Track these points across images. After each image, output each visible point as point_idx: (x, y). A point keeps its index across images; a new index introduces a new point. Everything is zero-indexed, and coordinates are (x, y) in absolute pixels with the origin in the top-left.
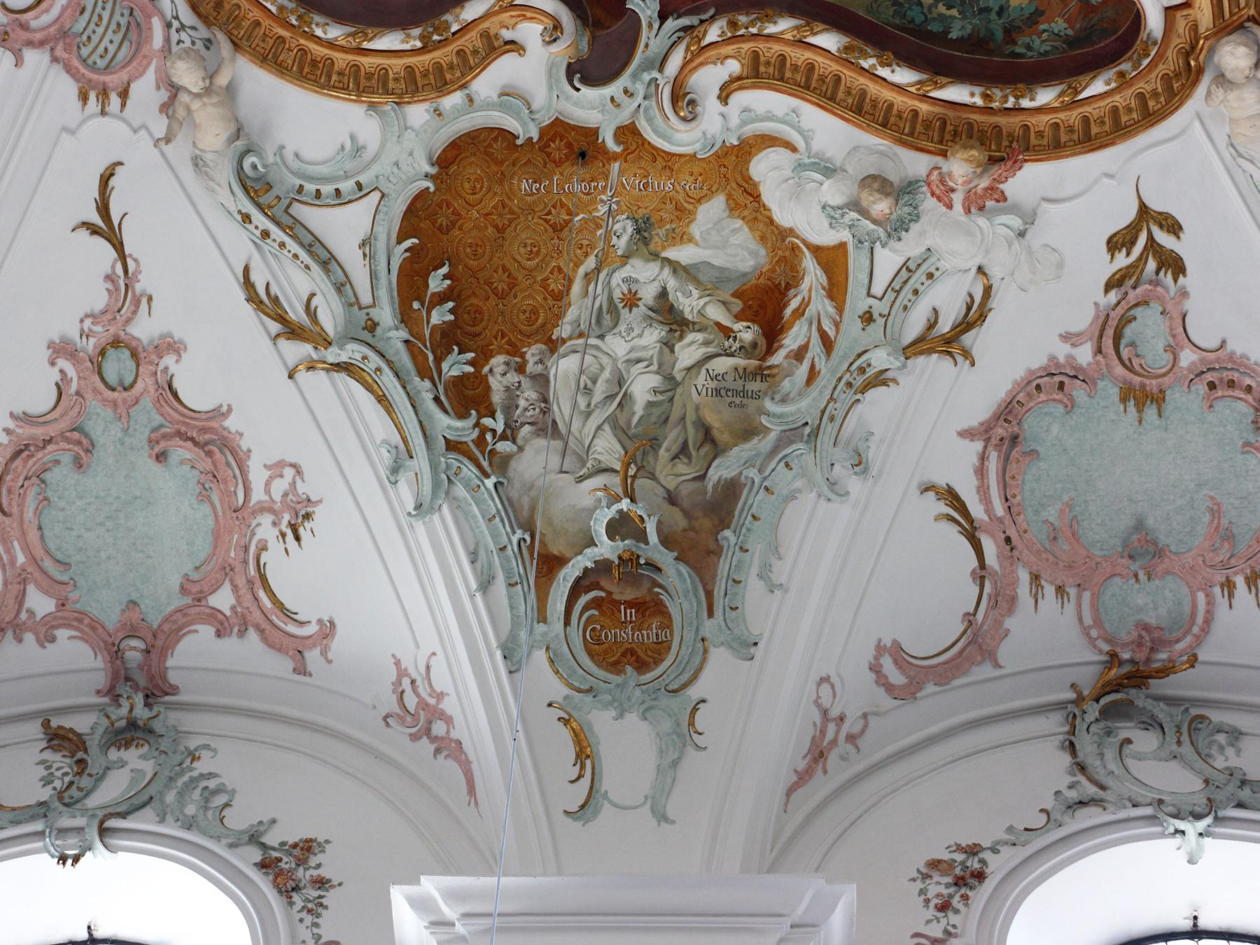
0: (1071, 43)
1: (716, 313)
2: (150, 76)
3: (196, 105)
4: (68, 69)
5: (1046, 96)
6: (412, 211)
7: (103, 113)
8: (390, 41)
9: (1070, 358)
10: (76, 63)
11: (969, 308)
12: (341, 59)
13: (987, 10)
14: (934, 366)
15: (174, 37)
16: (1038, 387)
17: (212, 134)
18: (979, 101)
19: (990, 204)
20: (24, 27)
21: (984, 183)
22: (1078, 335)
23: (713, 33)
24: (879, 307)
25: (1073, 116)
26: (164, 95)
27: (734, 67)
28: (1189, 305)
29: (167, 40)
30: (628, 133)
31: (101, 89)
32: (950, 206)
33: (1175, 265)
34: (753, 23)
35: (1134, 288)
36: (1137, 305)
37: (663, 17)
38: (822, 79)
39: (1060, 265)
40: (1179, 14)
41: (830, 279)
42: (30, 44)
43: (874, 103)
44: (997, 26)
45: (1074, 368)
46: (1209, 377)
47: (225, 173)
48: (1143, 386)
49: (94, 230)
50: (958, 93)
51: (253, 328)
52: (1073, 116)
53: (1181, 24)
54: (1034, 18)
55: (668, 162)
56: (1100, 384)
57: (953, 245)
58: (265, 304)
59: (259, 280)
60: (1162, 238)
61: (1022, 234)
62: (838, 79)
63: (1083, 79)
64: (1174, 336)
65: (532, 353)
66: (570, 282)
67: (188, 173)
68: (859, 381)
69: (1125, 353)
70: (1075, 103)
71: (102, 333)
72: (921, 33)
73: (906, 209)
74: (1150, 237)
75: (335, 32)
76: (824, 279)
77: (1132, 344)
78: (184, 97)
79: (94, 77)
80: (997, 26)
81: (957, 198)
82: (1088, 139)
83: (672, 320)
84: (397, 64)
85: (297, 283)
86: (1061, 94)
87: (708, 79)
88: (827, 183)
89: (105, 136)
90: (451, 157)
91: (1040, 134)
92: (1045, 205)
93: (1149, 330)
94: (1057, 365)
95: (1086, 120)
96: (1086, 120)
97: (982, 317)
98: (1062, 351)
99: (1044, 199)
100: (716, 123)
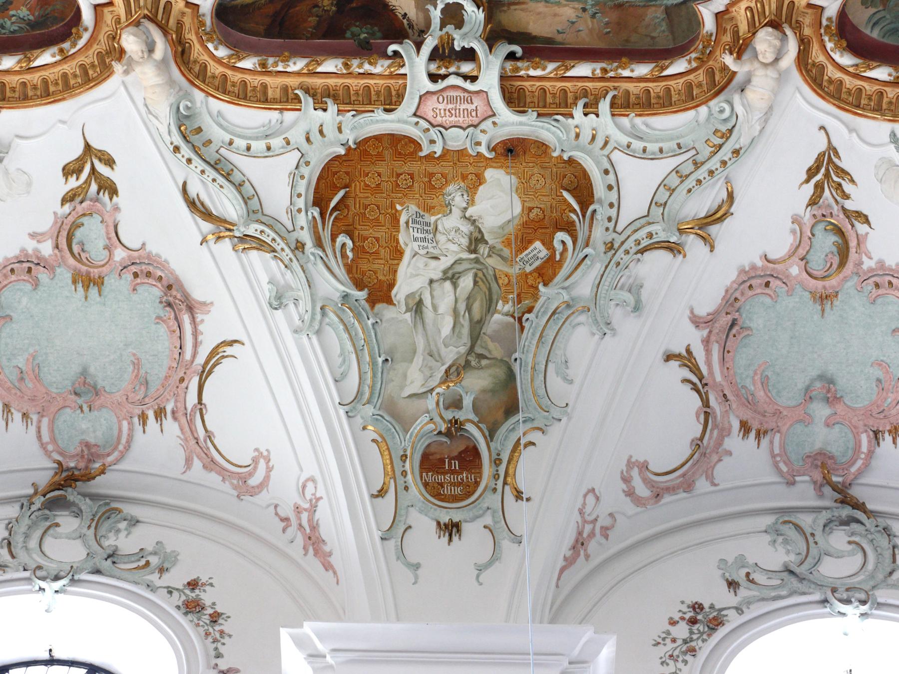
0: (33, 25)
9: (36, 251)
16: (12, 270)
22: (42, 234)
25: (35, 78)
28: (121, 217)
35: (81, 202)
36: (84, 215)
39: (29, 184)
40: (106, 10)
45: (38, 258)
46: (134, 269)
48: (88, 273)
53: (108, 17)
56: (58, 270)
60: (101, 168)
63: (36, 52)
64: (109, 239)
69: (76, 249)
74: (93, 169)
77: (82, 244)
82: (47, 93)
86: (19, 62)
91: (13, 90)
93: (93, 233)
94: (27, 255)
95: (45, 82)
96: (45, 82)
98: (30, 246)
99: (17, 136)
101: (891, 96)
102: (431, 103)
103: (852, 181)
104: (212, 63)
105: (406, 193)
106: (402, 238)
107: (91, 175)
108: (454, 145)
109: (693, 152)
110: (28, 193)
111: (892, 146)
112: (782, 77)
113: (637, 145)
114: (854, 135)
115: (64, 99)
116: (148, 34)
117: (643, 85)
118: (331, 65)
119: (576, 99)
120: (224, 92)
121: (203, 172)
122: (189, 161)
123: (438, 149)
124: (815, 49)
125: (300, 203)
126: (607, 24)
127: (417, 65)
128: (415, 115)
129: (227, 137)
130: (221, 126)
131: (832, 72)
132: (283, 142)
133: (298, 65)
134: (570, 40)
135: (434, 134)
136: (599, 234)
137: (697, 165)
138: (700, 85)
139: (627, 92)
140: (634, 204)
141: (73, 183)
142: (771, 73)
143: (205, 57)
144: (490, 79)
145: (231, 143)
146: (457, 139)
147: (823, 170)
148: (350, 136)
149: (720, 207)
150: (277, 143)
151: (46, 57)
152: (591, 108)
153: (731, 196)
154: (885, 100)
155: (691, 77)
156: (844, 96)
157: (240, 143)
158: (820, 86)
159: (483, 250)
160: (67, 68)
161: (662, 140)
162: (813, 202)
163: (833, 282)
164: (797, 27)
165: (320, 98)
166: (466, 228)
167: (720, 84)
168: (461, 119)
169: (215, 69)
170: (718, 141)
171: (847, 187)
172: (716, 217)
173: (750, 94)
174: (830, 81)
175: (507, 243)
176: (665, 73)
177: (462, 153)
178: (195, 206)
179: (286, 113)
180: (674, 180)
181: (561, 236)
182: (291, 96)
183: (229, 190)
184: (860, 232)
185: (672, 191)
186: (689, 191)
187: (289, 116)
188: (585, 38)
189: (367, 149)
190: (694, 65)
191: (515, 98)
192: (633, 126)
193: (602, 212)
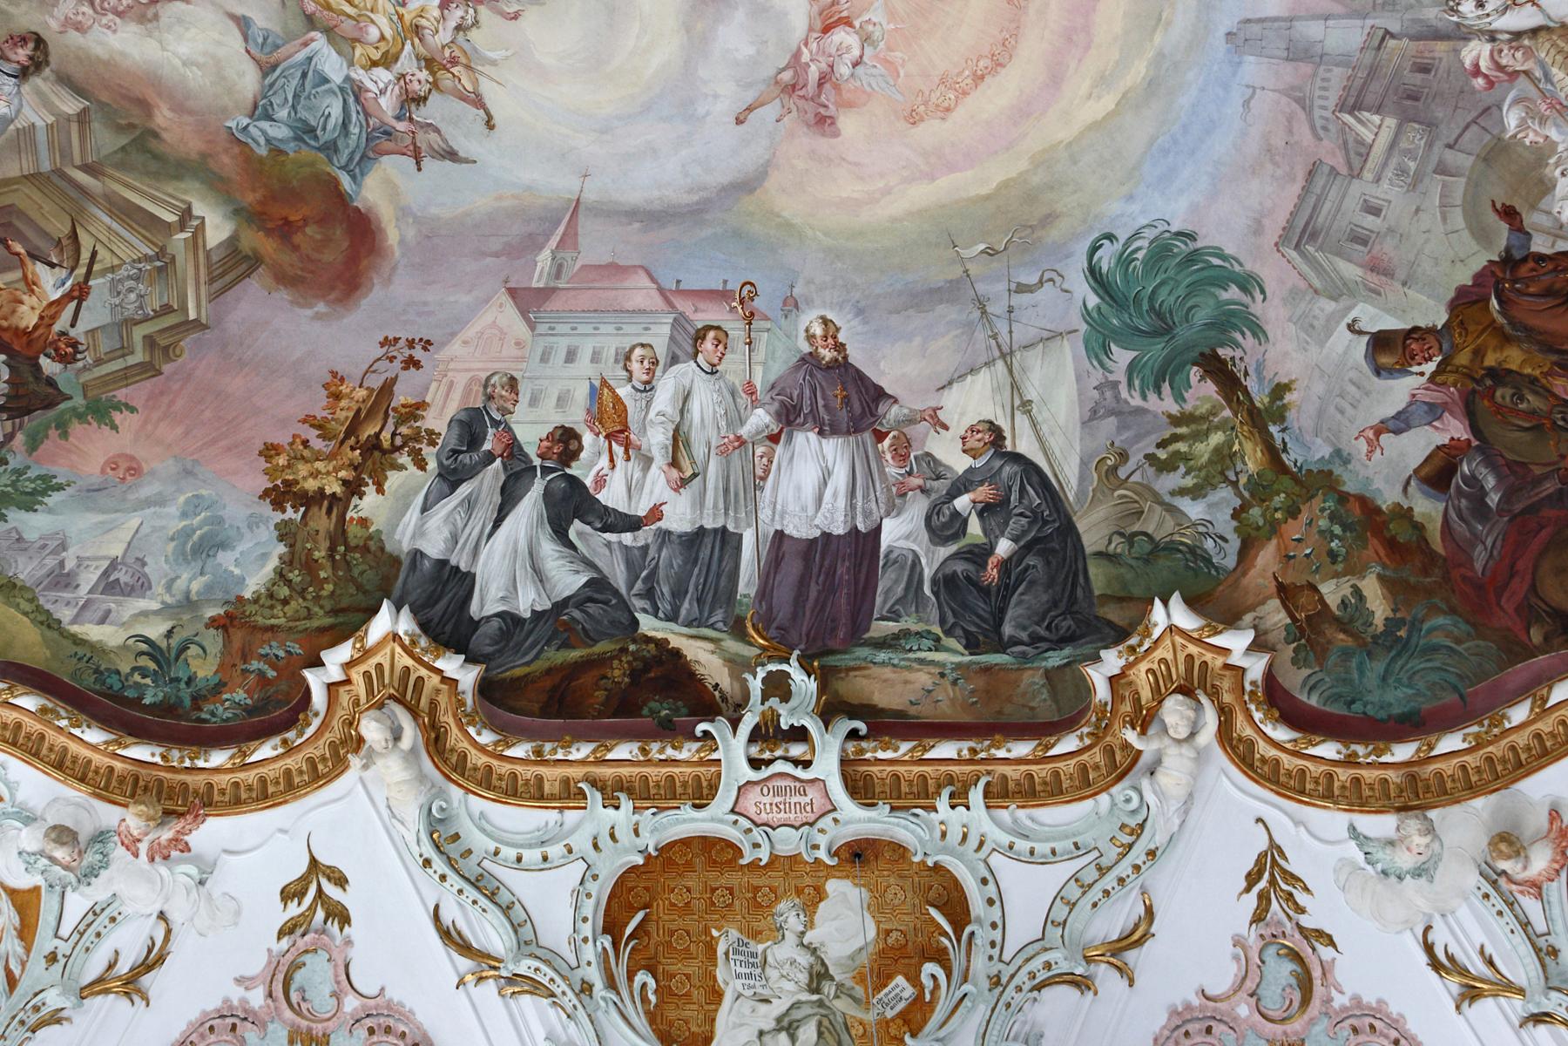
0: (250, 711)
5: (218, 758)
9: (244, 1001)
11: (150, 951)
13: (178, 680)
14: (111, 1005)
16: (211, 1028)
18: (158, 759)
19: (175, 854)
21: (166, 834)
22: (252, 979)
24: (63, 948)
25: (251, 776)
28: (355, 954)
32: (136, 855)
33: (342, 916)
35: (303, 935)
36: (306, 952)
38: (28, 736)
39: (238, 913)
40: (342, 690)
41: (22, 920)
43: (75, 759)
44: (186, 694)
45: (245, 1011)
46: (369, 1022)
48: (310, 1030)
52: (251, 776)
53: (344, 697)
54: (218, 688)
56: (271, 1027)
57: (136, 890)
60: (330, 890)
61: (201, 883)
62: (42, 737)
64: (338, 983)
68: (33, 1019)
69: (294, 997)
72: (118, 698)
73: (99, 857)
74: (320, 890)
76: (16, 921)
77: (302, 990)
80: (186, 694)
81: (143, 847)
82: (264, 795)
86: (231, 758)
88: (25, 831)
91: (222, 792)
92: (225, 856)
93: (317, 976)
94: (231, 1007)
95: (263, 781)
96: (263, 781)
97: (161, 959)
98: (236, 994)
99: (225, 851)
101: (1343, 778)
102: (754, 796)
103: (1306, 889)
104: (474, 751)
105: (724, 913)
106: (720, 974)
107: (317, 896)
108: (784, 849)
109: (1095, 854)
110: (236, 924)
111: (1353, 843)
112: (1201, 757)
113: (1022, 845)
114: (1302, 829)
115: (286, 802)
116: (392, 717)
117: (1023, 768)
118: (624, 751)
119: (939, 787)
120: (489, 788)
121: (460, 892)
122: (443, 878)
123: (764, 855)
124: (1240, 721)
125: (587, 930)
126: (973, 692)
127: (734, 748)
128: (732, 811)
129: (492, 846)
130: (483, 831)
131: (1264, 749)
132: (563, 851)
133: (582, 751)
134: (926, 712)
135: (757, 835)
136: (980, 964)
137: (1102, 871)
138: (1097, 767)
139: (1004, 777)
140: (1023, 925)
141: (294, 910)
142: (1186, 750)
143: (464, 745)
144: (827, 766)
145: (496, 853)
146: (788, 842)
147: (1266, 875)
148: (650, 841)
149: (1136, 926)
150: (556, 851)
151: (266, 750)
152: (959, 798)
153: (1150, 912)
154: (1336, 784)
155: (1085, 757)
156: (1282, 779)
158: (1251, 766)
159: (828, 988)
160: (291, 762)
161: (1054, 839)
162: (1258, 917)
163: (1296, 1026)
164: (1214, 694)
165: (611, 792)
166: (804, 959)
167: (1122, 765)
168: (792, 816)
169: (477, 759)
170: (1127, 839)
171: (1301, 898)
172: (1136, 937)
173: (1162, 778)
174: (1264, 760)
175: (860, 979)
176: (1051, 753)
177: (795, 859)
178: (448, 935)
179: (567, 812)
180: (1074, 892)
181: (930, 968)
182: (573, 790)
183: (495, 914)
184: (1324, 958)
185: (1072, 906)
186: (1095, 905)
187: (572, 816)
188: (946, 706)
189: (672, 858)
190: (1087, 741)
191: (860, 788)
192: (1015, 821)
193: (983, 935)
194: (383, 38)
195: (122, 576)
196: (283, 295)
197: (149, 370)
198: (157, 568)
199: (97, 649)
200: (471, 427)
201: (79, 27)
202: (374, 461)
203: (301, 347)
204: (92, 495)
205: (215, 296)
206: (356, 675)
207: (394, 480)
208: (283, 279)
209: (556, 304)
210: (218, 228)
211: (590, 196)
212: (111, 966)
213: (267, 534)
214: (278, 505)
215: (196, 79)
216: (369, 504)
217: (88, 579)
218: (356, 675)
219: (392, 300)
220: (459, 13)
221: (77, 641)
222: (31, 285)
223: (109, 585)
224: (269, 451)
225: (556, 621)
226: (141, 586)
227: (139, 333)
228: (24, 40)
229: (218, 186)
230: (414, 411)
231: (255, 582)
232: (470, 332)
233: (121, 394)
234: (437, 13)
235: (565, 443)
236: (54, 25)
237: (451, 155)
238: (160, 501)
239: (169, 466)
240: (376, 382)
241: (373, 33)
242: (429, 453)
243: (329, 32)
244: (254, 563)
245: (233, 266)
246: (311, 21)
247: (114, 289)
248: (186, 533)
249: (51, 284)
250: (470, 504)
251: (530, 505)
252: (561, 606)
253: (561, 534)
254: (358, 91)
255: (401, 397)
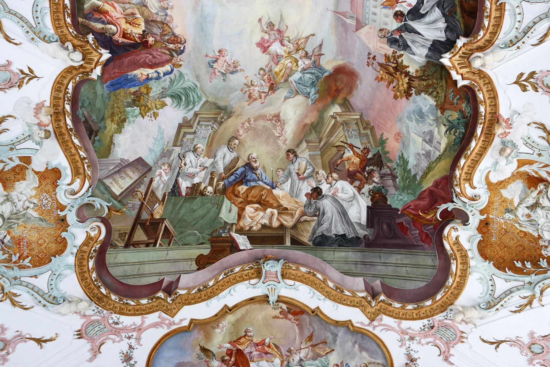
0: (469, 102)
1: (535, 194)
2: (458, 325)
3: (467, 316)
4: (455, 344)
5: (482, 109)
6: (498, 268)
7: (467, 338)
8: (454, 267)
10: (454, 342)
11: (539, 128)
12: (458, 279)
13: (458, 123)
15: (449, 318)
17: (474, 314)
18: (482, 125)
19: (510, 122)
20: (444, 352)
21: (504, 124)
23: (458, 190)
24: (537, 152)
25: (488, 101)
26: (463, 323)
27: (467, 185)
28: (545, 69)
29: (450, 319)
30: (482, 212)
31: (461, 338)
32: (510, 133)
33: (532, 74)
34: (456, 181)
37: (453, 202)
38: (472, 164)
39: (529, 104)
40: (464, 76)
41: (527, 164)
42: (449, 352)
43: (480, 151)
44: (462, 120)
47: (485, 313)
49: (498, 346)
50: (479, 130)
51: (527, 312)
52: (488, 101)
53: (467, 76)
54: (461, 111)
55: (490, 203)
58: (520, 309)
59: (514, 309)
60: (524, 78)
61: (519, 114)
62: (472, 160)
63: (478, 99)
65: (541, 243)
66: (521, 231)
67: (483, 321)
70: (485, 101)
71: (526, 351)
73: (509, 143)
75: (451, 280)
76: (527, 166)
78: (464, 319)
79: (457, 338)
80: (462, 120)
81: (507, 131)
82: (494, 98)
83: (535, 206)
84: (460, 266)
85: (516, 300)
87: (469, 192)
88: (500, 164)
89: (473, 338)
90: (485, 256)
91: (492, 109)
92: (511, 108)
97: (542, 125)
100: (482, 191)
104: (485, 38)
110: (533, 104)
120: (496, 32)
121: (528, 37)
122: (523, 43)
129: (514, 30)
130: (509, 33)
143: (483, 40)
145: (517, 28)
150: (518, 11)
151: (480, 96)
157: (517, 25)
160: (485, 89)
169: (487, 37)
179: (506, 9)
182: (499, 7)
194: (291, 62)
195: (427, 138)
196: (355, 92)
197: (372, 129)
198: (426, 128)
199: (448, 145)
200: (392, 42)
201: (285, 141)
202: (400, 69)
203: (368, 88)
204: (405, 145)
205: (354, 111)
206: (461, 71)
207: (405, 63)
208: (350, 92)
209: (360, 18)
210: (336, 109)
211: (332, 8)
212: (544, 138)
213: (418, 98)
214: (410, 95)
215: (299, 111)
216: (412, 70)
217: (428, 147)
218: (461, 71)
219: (357, 63)
220: (285, 41)
221: (445, 150)
222: (349, 159)
223: (430, 142)
224: (396, 97)
225: (448, 16)
226: (431, 133)
227: (363, 131)
228: (288, 155)
229: (326, 108)
230: (387, 57)
231: (431, 101)
232: (367, 42)
233: (378, 137)
234: (285, 47)
235: (398, 15)
236: (285, 147)
237: (321, 45)
238: (407, 128)
239: (398, 125)
240: (378, 68)
241: (290, 64)
242: (399, 53)
243: (289, 76)
244: (426, 102)
245: (346, 105)
246: (286, 81)
247: (351, 137)
248: (417, 120)
249: (348, 154)
250: (413, 42)
251: (415, 25)
252: (444, 15)
253: (423, 16)
254: (304, 70)
255: (383, 61)
